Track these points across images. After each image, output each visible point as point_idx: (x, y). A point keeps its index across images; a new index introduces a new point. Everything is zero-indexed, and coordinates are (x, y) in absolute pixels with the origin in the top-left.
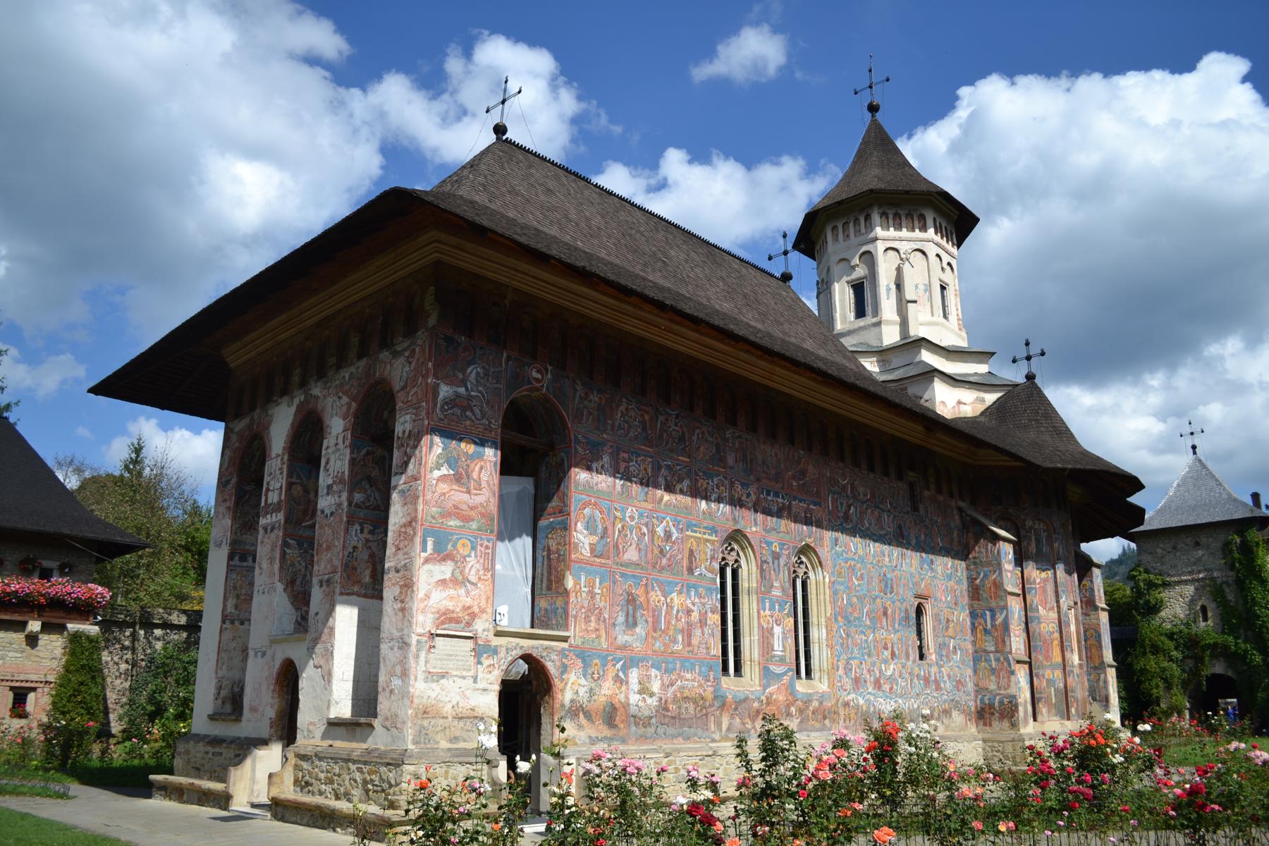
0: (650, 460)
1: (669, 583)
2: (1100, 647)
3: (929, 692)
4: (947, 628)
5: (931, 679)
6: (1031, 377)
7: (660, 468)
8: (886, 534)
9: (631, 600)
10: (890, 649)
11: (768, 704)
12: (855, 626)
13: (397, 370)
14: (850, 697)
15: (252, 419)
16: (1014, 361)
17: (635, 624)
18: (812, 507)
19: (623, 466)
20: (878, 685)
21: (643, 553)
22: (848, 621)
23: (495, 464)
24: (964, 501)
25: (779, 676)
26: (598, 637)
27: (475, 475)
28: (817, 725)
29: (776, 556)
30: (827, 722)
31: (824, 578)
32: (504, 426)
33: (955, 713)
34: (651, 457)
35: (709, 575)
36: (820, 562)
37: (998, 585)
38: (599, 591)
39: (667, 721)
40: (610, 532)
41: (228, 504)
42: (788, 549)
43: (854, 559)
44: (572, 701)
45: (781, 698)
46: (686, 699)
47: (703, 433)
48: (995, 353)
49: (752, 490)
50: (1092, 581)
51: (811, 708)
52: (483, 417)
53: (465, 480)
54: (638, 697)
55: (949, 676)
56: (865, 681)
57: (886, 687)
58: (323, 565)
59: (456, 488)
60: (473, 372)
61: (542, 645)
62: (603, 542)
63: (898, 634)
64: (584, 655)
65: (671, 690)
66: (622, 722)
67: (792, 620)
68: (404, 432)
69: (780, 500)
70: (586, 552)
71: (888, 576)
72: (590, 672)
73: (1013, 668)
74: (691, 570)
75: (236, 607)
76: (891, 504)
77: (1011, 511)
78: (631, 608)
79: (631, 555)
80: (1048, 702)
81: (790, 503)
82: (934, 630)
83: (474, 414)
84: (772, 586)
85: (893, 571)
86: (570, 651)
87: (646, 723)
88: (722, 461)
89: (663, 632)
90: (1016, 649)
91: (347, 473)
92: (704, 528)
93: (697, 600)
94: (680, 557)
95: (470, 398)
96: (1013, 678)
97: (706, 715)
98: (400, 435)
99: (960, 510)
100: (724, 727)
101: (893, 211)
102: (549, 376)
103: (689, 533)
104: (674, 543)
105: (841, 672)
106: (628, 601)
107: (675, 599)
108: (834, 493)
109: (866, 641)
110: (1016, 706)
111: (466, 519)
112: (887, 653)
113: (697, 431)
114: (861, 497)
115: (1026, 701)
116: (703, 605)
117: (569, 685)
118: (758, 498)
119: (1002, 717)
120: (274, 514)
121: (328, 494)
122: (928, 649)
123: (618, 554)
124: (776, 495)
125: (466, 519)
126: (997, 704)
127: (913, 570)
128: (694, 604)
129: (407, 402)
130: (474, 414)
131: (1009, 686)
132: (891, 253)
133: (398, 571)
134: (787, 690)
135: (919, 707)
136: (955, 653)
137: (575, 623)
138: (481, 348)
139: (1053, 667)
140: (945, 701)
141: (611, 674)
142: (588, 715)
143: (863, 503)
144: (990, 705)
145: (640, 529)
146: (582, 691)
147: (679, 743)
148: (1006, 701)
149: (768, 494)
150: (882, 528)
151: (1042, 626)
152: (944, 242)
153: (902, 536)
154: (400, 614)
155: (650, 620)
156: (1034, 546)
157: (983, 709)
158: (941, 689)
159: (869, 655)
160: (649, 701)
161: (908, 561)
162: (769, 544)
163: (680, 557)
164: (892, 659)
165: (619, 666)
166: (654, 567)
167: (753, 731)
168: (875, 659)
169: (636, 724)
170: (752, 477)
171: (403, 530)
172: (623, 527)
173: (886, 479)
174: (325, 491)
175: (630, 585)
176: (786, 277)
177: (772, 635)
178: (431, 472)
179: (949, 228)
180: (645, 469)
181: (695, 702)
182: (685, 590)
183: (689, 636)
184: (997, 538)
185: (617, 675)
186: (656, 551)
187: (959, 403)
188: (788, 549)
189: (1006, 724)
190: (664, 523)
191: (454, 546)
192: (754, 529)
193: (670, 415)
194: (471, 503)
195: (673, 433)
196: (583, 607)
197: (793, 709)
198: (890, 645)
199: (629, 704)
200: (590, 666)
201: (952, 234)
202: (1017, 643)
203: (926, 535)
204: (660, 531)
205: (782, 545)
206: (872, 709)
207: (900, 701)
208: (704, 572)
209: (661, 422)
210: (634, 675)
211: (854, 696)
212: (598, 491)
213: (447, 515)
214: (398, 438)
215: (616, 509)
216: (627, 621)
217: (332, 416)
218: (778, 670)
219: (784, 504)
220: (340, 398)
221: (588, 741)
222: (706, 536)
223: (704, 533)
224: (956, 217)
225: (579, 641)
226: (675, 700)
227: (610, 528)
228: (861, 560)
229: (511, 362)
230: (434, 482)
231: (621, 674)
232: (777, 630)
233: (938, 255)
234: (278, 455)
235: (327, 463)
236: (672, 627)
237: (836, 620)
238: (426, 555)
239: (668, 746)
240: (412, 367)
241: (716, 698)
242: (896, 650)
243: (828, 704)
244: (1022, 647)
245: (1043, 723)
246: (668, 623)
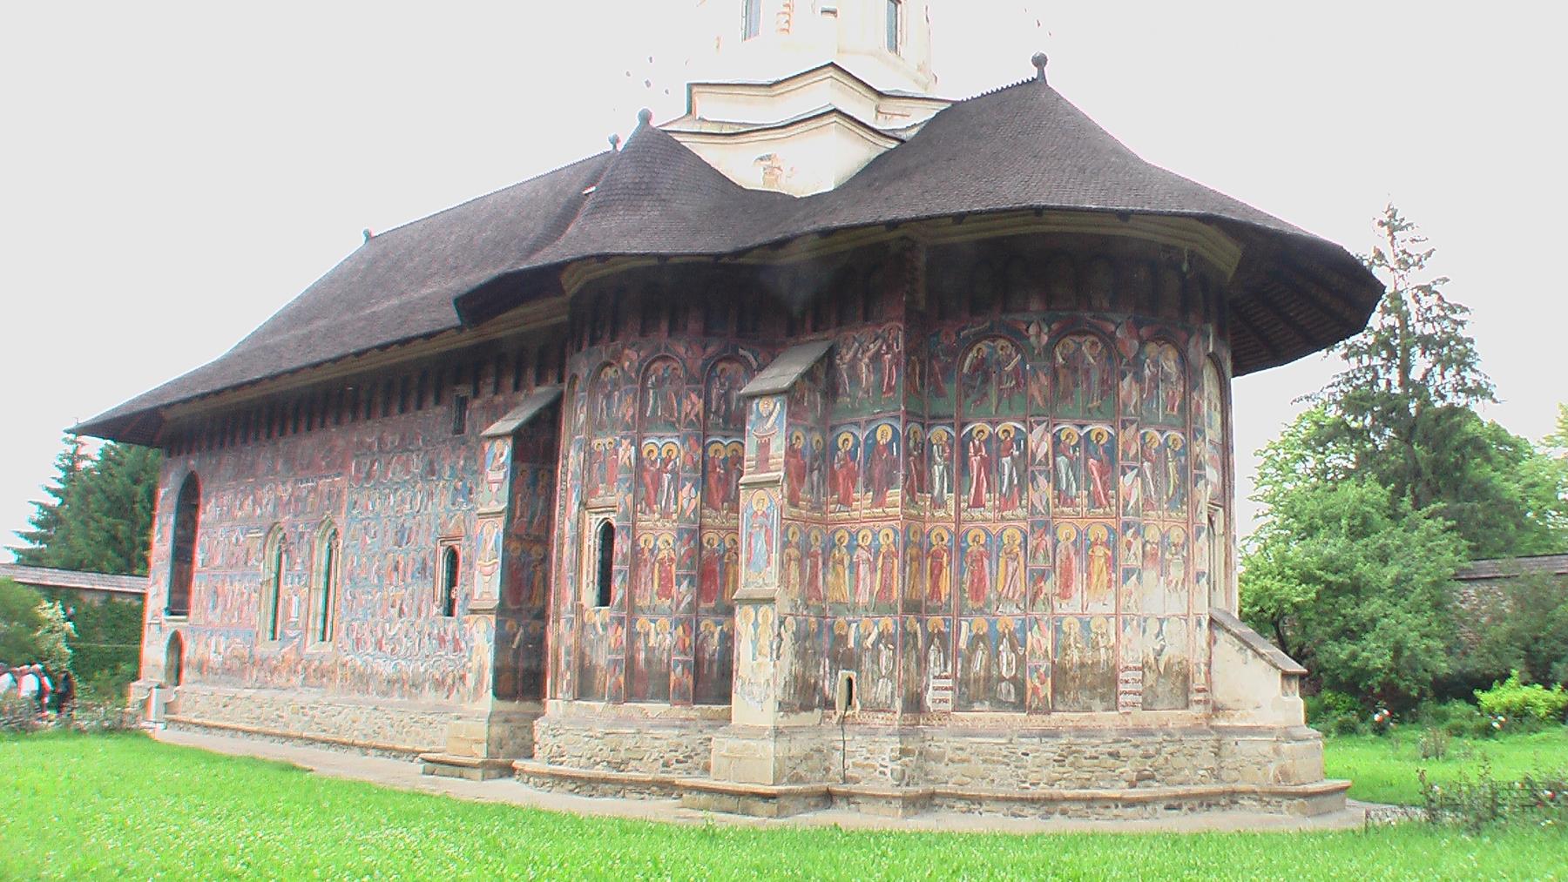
3: (443, 653)
5: (447, 638)
9: (216, 592)
10: (398, 607)
14: (348, 658)
18: (337, 479)
20: (379, 645)
28: (317, 683)
29: (302, 535)
30: (325, 680)
35: (256, 564)
46: (236, 657)
51: (313, 667)
56: (365, 643)
57: (387, 648)
65: (229, 650)
67: (307, 589)
74: (246, 563)
79: (219, 561)
85: (414, 517)
90: (481, 595)
103: (248, 536)
112: (394, 612)
115: (481, 667)
135: (426, 671)
141: (204, 641)
143: (388, 453)
150: (408, 472)
153: (433, 472)
158: (461, 650)
162: (296, 527)
164: (400, 616)
177: (290, 604)
197: (300, 667)
198: (399, 602)
207: (403, 663)
210: (214, 640)
232: (295, 599)
242: (404, 606)
243: (326, 664)
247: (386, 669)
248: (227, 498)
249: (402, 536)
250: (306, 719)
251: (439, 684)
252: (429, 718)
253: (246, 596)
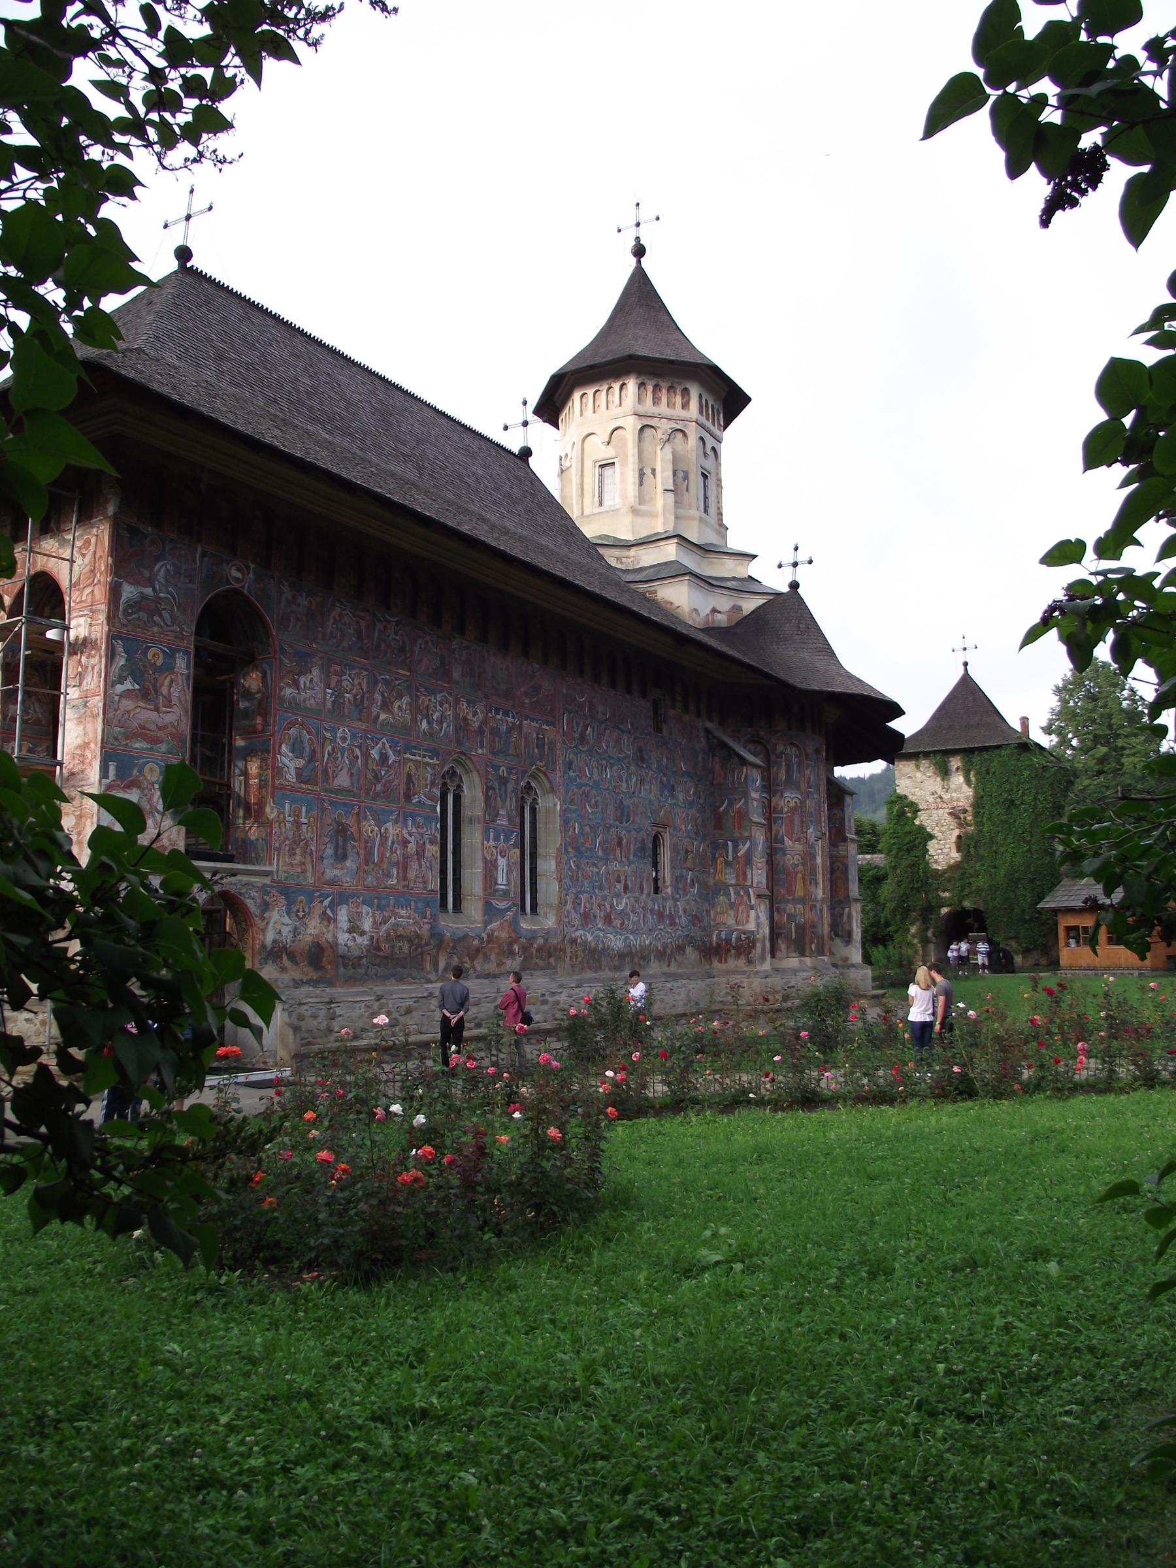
0: (365, 673)
1: (384, 811)
2: (846, 880)
4: (686, 859)
6: (794, 586)
7: (376, 682)
8: (624, 758)
9: (341, 831)
11: (489, 941)
12: (587, 857)
14: (578, 934)
16: (780, 566)
17: (345, 857)
18: (545, 727)
19: (334, 679)
20: (608, 920)
21: (355, 778)
22: (579, 852)
23: (188, 677)
24: (711, 721)
25: (502, 912)
26: (304, 871)
27: (164, 690)
28: (542, 963)
29: (503, 782)
30: (552, 960)
31: (555, 805)
32: (198, 633)
33: (689, 950)
34: (367, 670)
35: (429, 802)
36: (552, 788)
37: (743, 815)
38: (305, 821)
39: (378, 961)
40: (319, 755)
42: (517, 773)
43: (588, 785)
44: (274, 941)
45: (504, 935)
46: (400, 937)
47: (426, 642)
48: (756, 556)
49: (480, 709)
50: (843, 810)
52: (173, 623)
53: (152, 696)
54: (347, 935)
55: (685, 910)
56: (595, 917)
57: (617, 923)
59: (141, 704)
60: (161, 570)
61: (240, 881)
62: (311, 766)
63: (633, 866)
64: (288, 892)
65: (384, 928)
66: (330, 963)
67: (518, 851)
69: (510, 719)
70: (291, 777)
71: (625, 803)
72: (294, 909)
73: (753, 902)
74: (408, 798)
76: (632, 724)
77: (762, 733)
78: (341, 839)
79: (343, 780)
80: (788, 939)
81: (521, 724)
82: (672, 861)
83: (163, 619)
84: (498, 814)
86: (272, 887)
87: (356, 962)
88: (446, 675)
89: (376, 865)
90: (759, 883)
92: (425, 750)
93: (414, 830)
94: (396, 782)
95: (158, 600)
96: (753, 913)
97: (422, 954)
99: (707, 731)
100: (442, 965)
101: (654, 382)
102: (251, 575)
103: (407, 756)
104: (390, 767)
105: (569, 906)
106: (338, 832)
107: (390, 829)
108: (570, 712)
109: (598, 873)
110: (754, 943)
111: (155, 741)
113: (420, 641)
114: (600, 716)
116: (422, 835)
117: (271, 924)
118: (486, 717)
119: (738, 956)
122: (664, 882)
123: (328, 780)
124: (506, 714)
125: (155, 741)
126: (733, 940)
127: (652, 797)
128: (411, 835)
129: (81, 602)
130: (163, 619)
131: (747, 921)
132: (648, 432)
134: (510, 926)
136: (692, 885)
137: (278, 856)
138: (172, 541)
139: (796, 901)
140: (679, 937)
142: (292, 957)
144: (726, 940)
145: (353, 752)
146: (286, 931)
147: (392, 987)
148: (743, 937)
149: (497, 713)
150: (621, 751)
151: (788, 857)
152: (709, 424)
153: (642, 759)
155: (362, 852)
156: (784, 772)
157: (718, 945)
158: (675, 924)
159: (600, 888)
160: (359, 940)
161: (647, 787)
162: (497, 768)
163: (396, 782)
165: (326, 902)
166: (368, 794)
167: (472, 971)
168: (606, 892)
169: (345, 966)
170: (480, 694)
171: (79, 752)
172: (333, 749)
173: (628, 696)
175: (340, 814)
176: (526, 453)
177: (496, 867)
178: (113, 686)
179: (716, 407)
180: (360, 684)
181: (410, 941)
182: (401, 819)
183: (405, 869)
184: (744, 762)
185: (324, 913)
186: (370, 776)
187: (714, 611)
188: (517, 773)
189: (742, 962)
190: (380, 744)
191: (141, 771)
192: (480, 751)
193: (389, 622)
194: (160, 722)
195: (393, 642)
196: (287, 838)
197: (516, 947)
199: (337, 944)
200: (294, 902)
201: (719, 413)
202: (758, 876)
203: (668, 759)
204: (375, 753)
205: (510, 770)
206: (601, 946)
208: (424, 799)
209: (380, 631)
210: (343, 914)
211: (582, 932)
212: (306, 708)
213: (133, 736)
215: (326, 729)
216: (336, 853)
218: (502, 905)
219: (514, 724)
221: (291, 984)
222: (427, 760)
223: (425, 756)
224: (724, 395)
225: (283, 876)
226: (388, 938)
227: (319, 750)
228: (597, 785)
229: (206, 559)
230: (117, 698)
231: (329, 912)
232: (502, 862)
233: (702, 439)
236: (386, 860)
237: (566, 851)
238: (108, 781)
239: (379, 989)
241: (432, 935)
244: (764, 881)
245: (781, 959)
246: (382, 856)
247: (616, 943)
248: (353, 683)
249: (623, 815)
250: (546, 1007)
251: (661, 955)
252: (669, 985)
253: (412, 847)
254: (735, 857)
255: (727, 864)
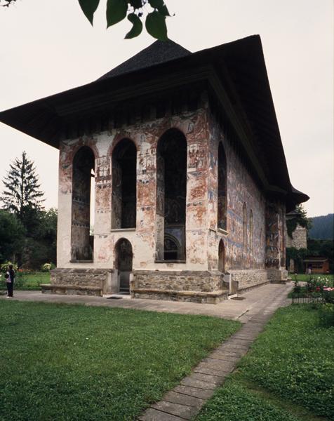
13: (186, 126)
15: (81, 140)
41: (68, 175)
58: (143, 202)
68: (193, 151)
75: (76, 218)
91: (155, 165)
98: (191, 151)
120: (105, 181)
121: (143, 174)
133: (195, 205)
154: (198, 222)
174: (141, 172)
189: (275, 268)
214: (190, 153)
217: (141, 142)
220: (146, 134)
234: (104, 156)
235: (142, 160)
240: (196, 124)
254: (274, 239)
255: (271, 241)
